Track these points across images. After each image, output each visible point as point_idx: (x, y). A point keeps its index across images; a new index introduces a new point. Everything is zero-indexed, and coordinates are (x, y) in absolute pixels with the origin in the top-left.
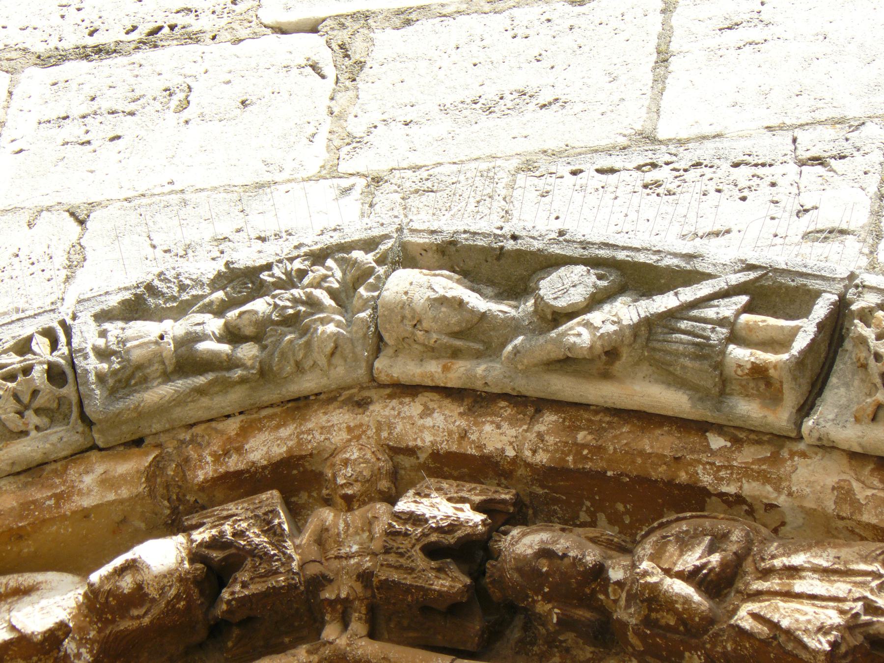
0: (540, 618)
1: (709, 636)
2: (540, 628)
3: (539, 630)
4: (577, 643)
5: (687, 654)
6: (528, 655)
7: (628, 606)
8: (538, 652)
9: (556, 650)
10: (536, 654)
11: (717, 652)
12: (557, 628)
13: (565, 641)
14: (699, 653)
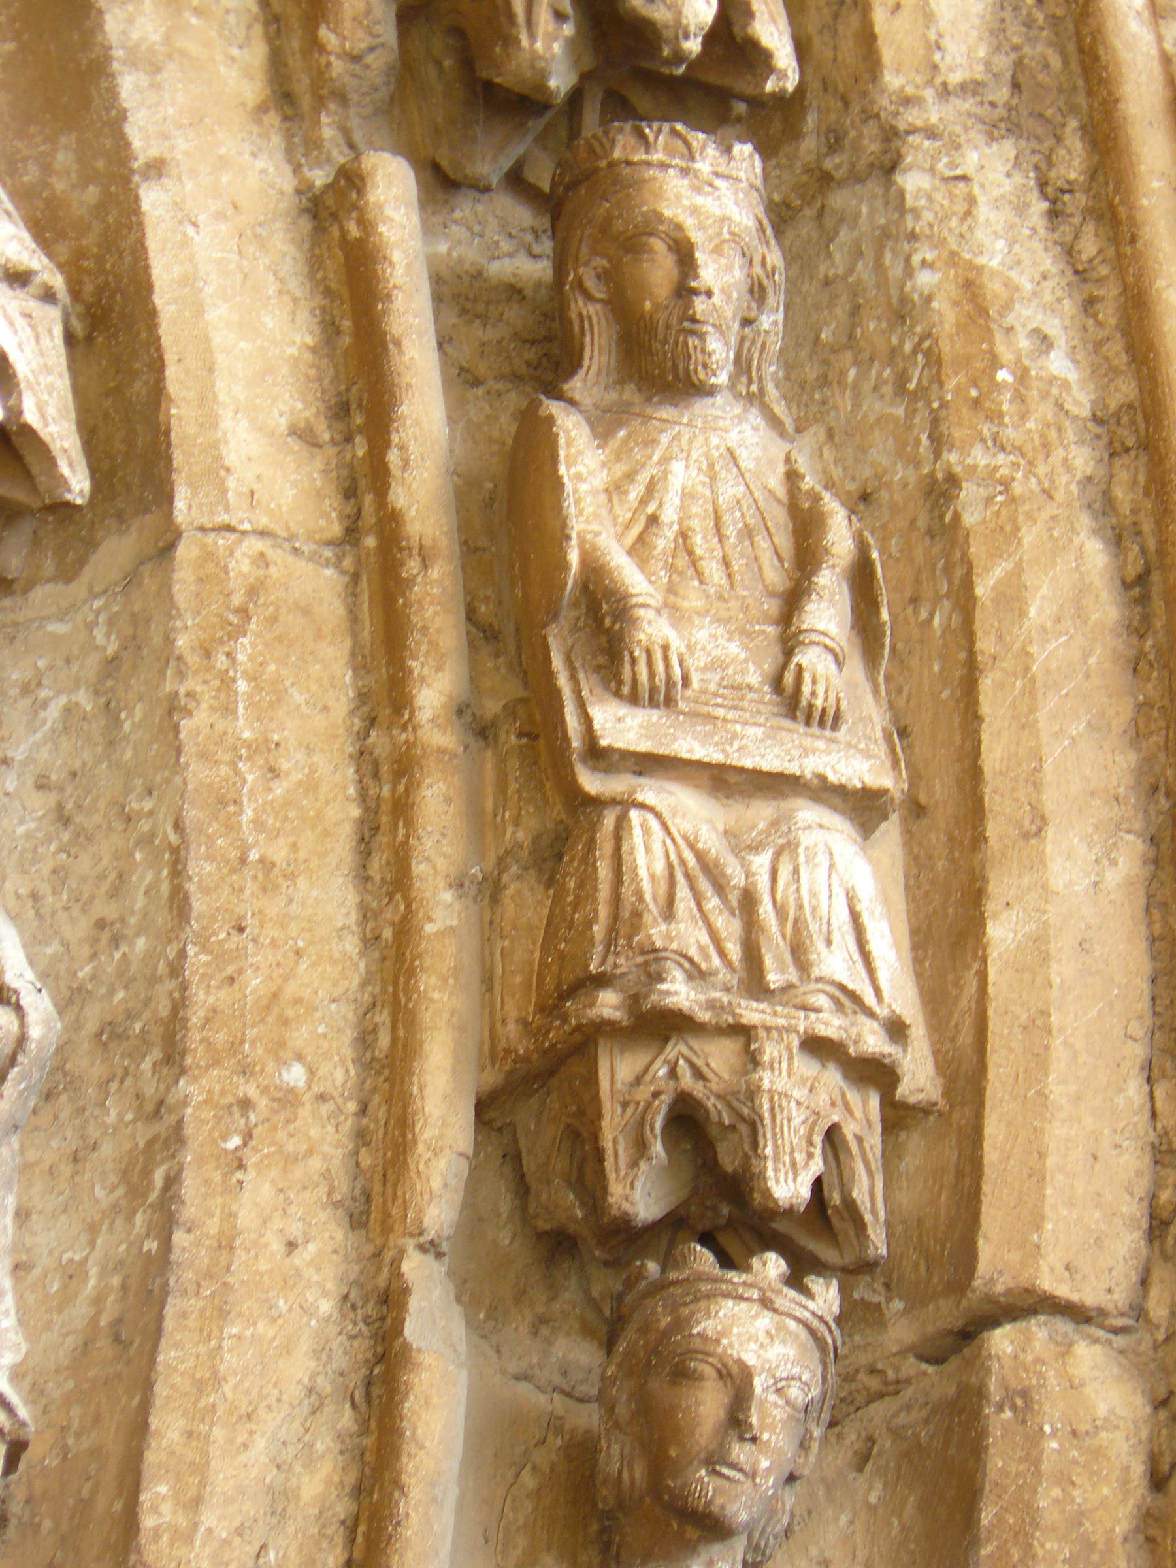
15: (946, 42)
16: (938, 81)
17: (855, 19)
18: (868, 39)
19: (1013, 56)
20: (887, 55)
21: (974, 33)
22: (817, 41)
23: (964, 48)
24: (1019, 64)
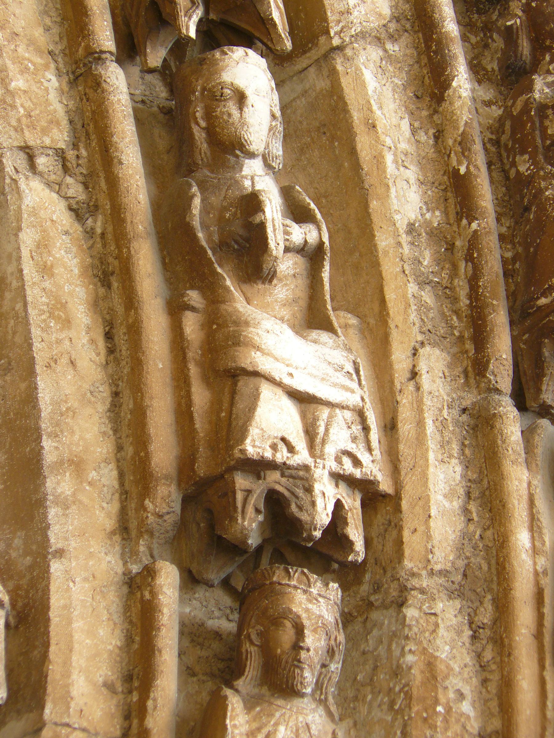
0: (505, 10)
1: (551, 170)
2: (497, 13)
3: (494, 12)
4: (496, 52)
5: (526, 157)
6: (467, 12)
7: (549, 85)
8: (473, 20)
9: (482, 35)
10: (470, 19)
11: (540, 183)
12: (503, 28)
13: (493, 40)
14: (532, 167)
15: (435, 550)
16: (429, 567)
17: (394, 533)
18: (399, 543)
19: (466, 561)
20: (407, 552)
21: (449, 548)
22: (375, 540)
23: (443, 554)
24: (468, 565)
